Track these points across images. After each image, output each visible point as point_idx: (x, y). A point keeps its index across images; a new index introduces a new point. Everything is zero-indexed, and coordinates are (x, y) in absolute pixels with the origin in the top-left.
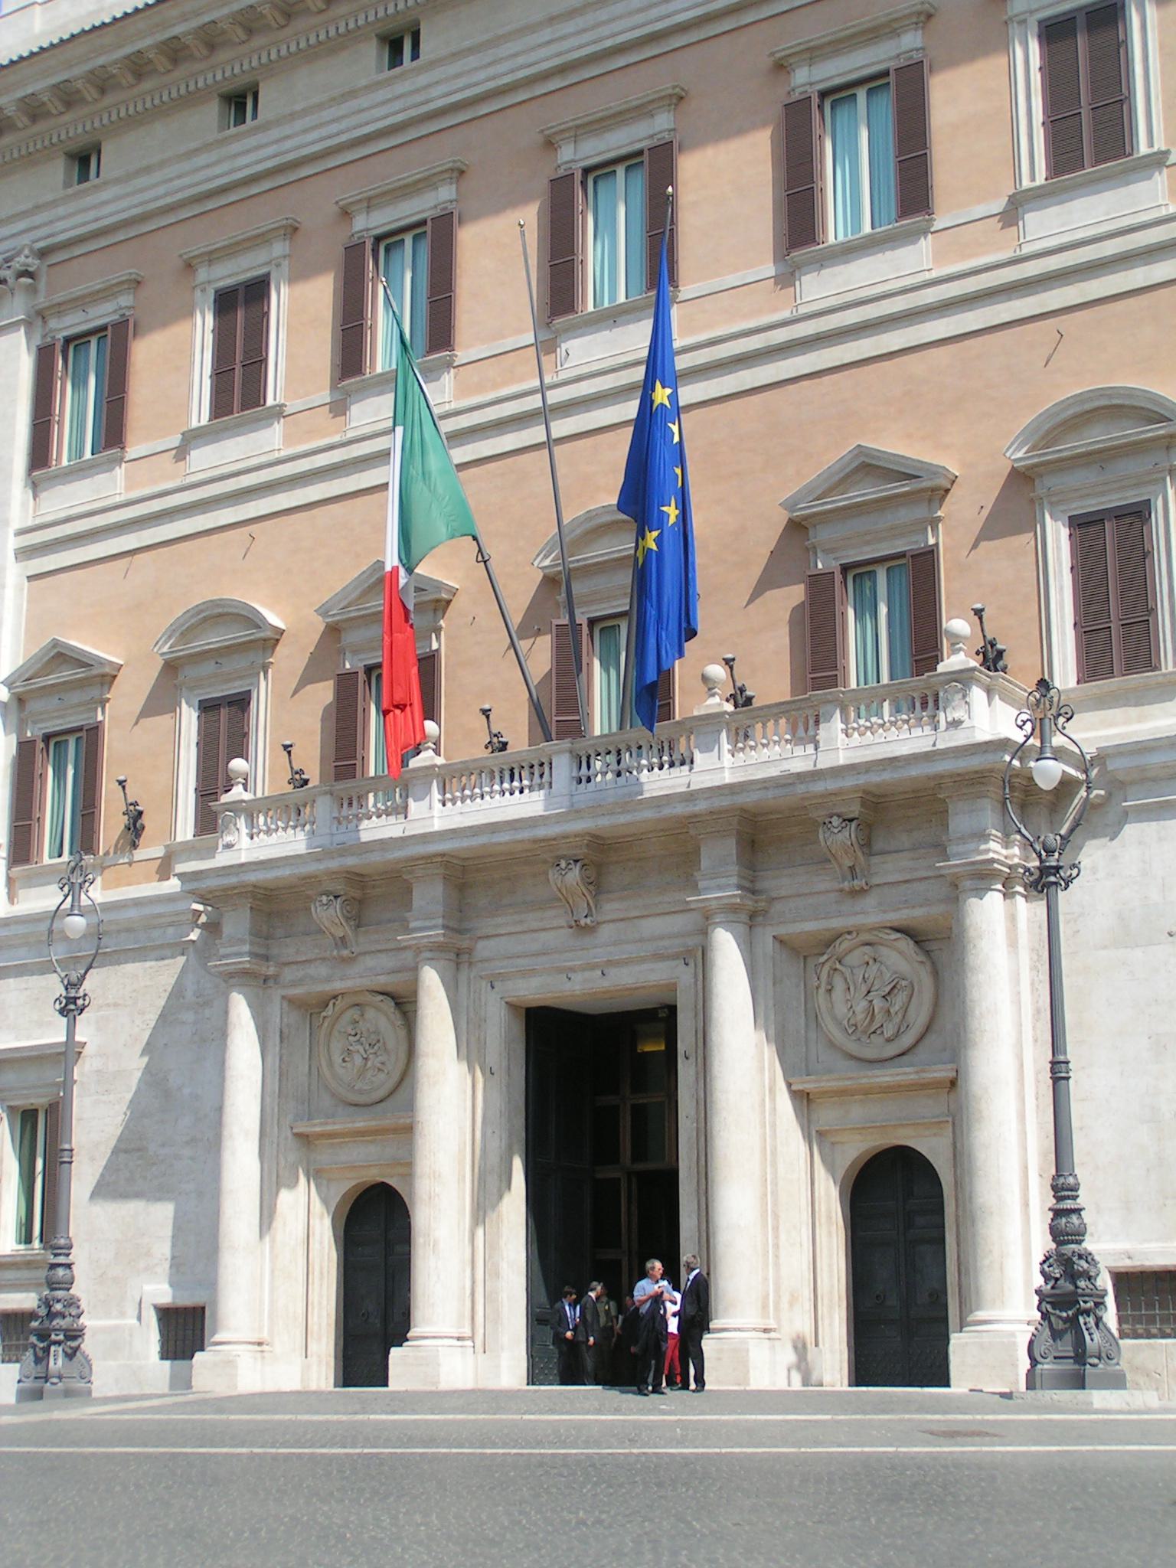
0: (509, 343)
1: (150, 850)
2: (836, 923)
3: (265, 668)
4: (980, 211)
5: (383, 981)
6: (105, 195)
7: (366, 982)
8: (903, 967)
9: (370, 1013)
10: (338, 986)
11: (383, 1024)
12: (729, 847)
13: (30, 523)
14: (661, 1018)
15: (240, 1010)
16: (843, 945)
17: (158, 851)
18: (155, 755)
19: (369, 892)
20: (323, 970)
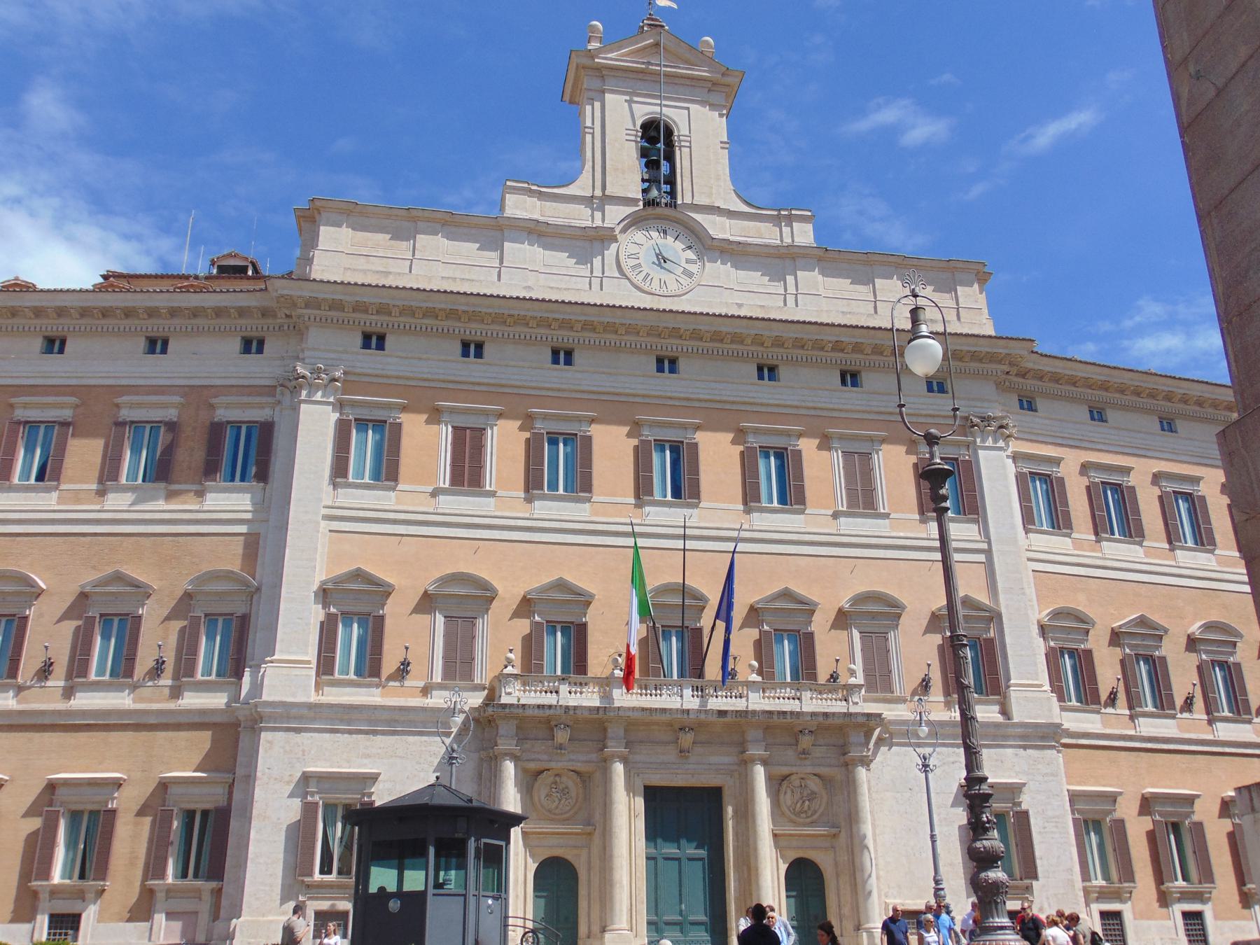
0: (619, 500)
1: (414, 682)
2: (794, 769)
3: (487, 612)
4: (823, 512)
5: (579, 767)
6: (389, 360)
7: (570, 765)
8: (815, 788)
9: (564, 779)
10: (553, 765)
11: (570, 784)
12: (759, 734)
13: (330, 503)
14: (713, 796)
15: (509, 768)
16: (793, 777)
17: (422, 684)
18: (415, 637)
19: (595, 728)
20: (545, 757)
